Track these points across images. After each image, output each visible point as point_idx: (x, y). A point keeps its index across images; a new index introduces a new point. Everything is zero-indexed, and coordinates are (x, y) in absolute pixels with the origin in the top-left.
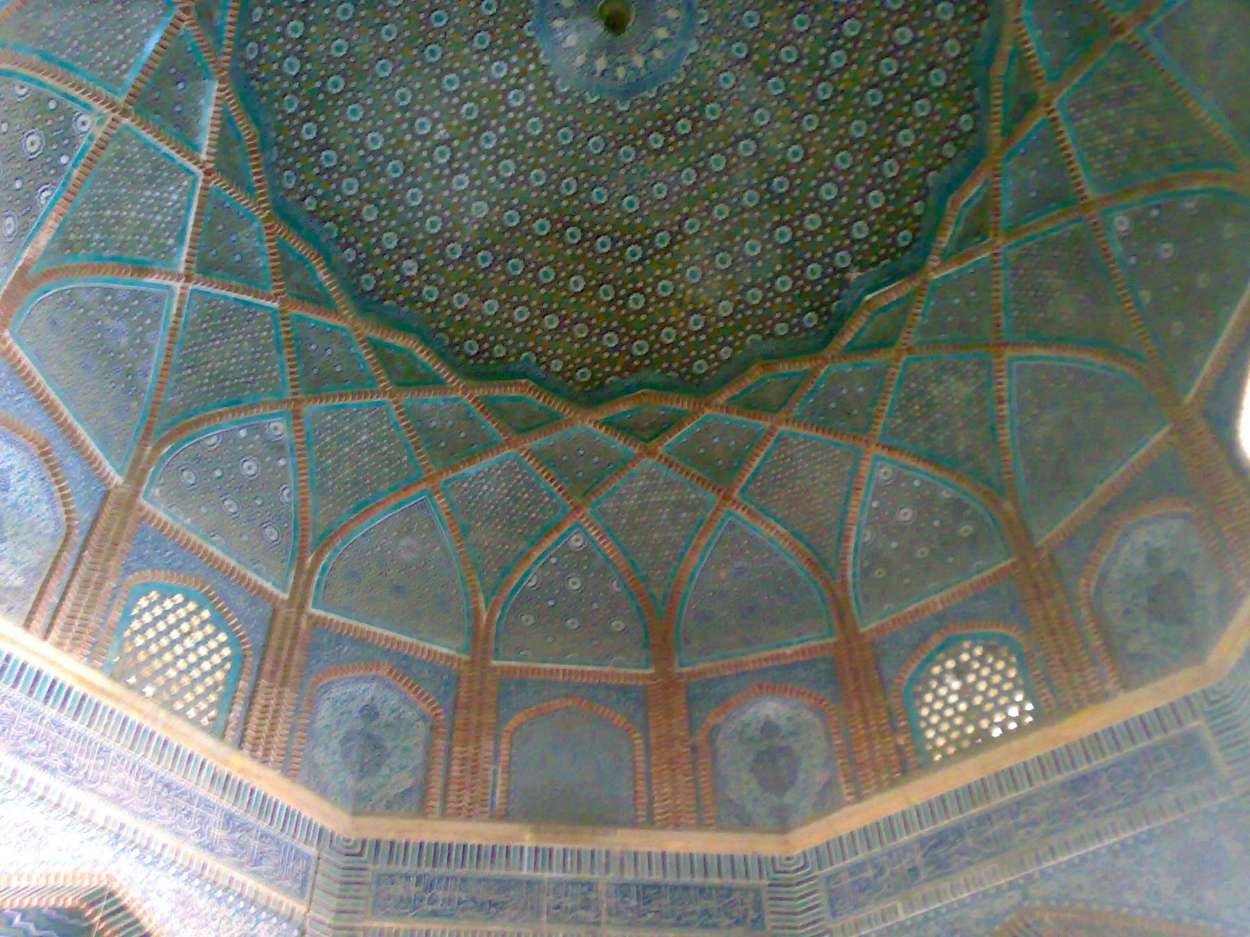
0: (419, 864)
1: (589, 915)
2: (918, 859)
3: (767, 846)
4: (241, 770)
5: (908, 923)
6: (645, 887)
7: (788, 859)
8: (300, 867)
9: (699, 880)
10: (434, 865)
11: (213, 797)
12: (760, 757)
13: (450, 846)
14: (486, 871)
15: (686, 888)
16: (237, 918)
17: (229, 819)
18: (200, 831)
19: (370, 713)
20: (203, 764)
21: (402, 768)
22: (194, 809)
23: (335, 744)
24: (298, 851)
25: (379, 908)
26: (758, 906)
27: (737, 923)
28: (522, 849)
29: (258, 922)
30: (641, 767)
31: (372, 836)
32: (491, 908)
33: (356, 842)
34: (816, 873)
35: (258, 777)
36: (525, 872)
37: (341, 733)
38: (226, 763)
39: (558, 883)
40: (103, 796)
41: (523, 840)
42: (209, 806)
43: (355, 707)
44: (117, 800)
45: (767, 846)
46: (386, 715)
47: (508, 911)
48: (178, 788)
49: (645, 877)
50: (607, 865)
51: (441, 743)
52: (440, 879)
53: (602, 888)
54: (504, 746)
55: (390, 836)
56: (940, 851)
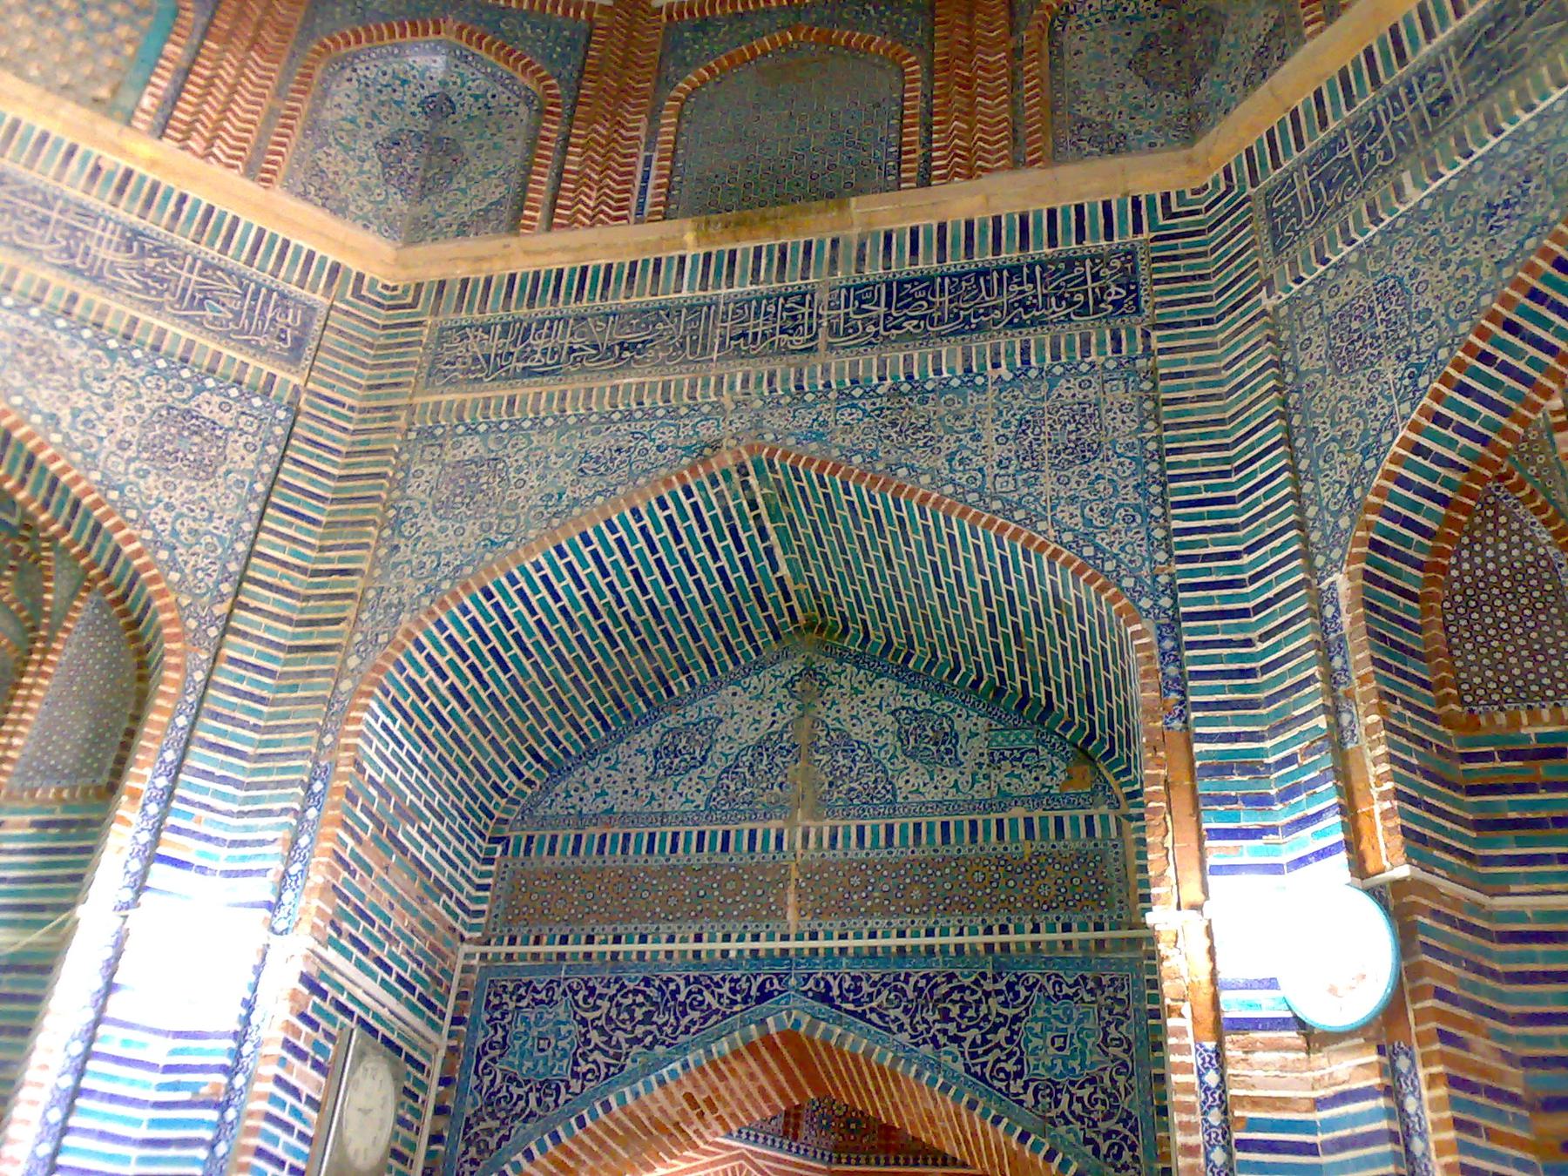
0: (506, 307)
1: (798, 341)
2: (1453, 76)
3: (1150, 174)
4: (153, 164)
5: (1426, 205)
6: (900, 283)
7: (1195, 192)
8: (293, 318)
9: (1010, 255)
10: (531, 305)
11: (98, 201)
12: (1149, 44)
13: (560, 273)
14: (619, 300)
15: (985, 272)
16: (151, 382)
17: (132, 239)
18: (68, 248)
19: (439, 106)
20: (71, 152)
21: (486, 175)
22: (55, 215)
23: (365, 147)
24: (283, 296)
25: (437, 373)
26: (1130, 284)
27: (1083, 310)
28: (682, 259)
29: (198, 392)
30: (915, 106)
31: (434, 274)
32: (626, 352)
33: (406, 291)
34: (1250, 191)
35: (194, 178)
36: (685, 293)
37: (382, 130)
38: (122, 151)
39: (742, 303)
41: (683, 246)
42: (85, 213)
43: (411, 97)
45: (1150, 174)
46: (467, 105)
47: (651, 354)
48: (17, 182)
49: (903, 267)
50: (833, 262)
51: (553, 130)
52: (542, 323)
53: (823, 296)
54: (668, 121)
55: (461, 271)
56: (1500, 43)
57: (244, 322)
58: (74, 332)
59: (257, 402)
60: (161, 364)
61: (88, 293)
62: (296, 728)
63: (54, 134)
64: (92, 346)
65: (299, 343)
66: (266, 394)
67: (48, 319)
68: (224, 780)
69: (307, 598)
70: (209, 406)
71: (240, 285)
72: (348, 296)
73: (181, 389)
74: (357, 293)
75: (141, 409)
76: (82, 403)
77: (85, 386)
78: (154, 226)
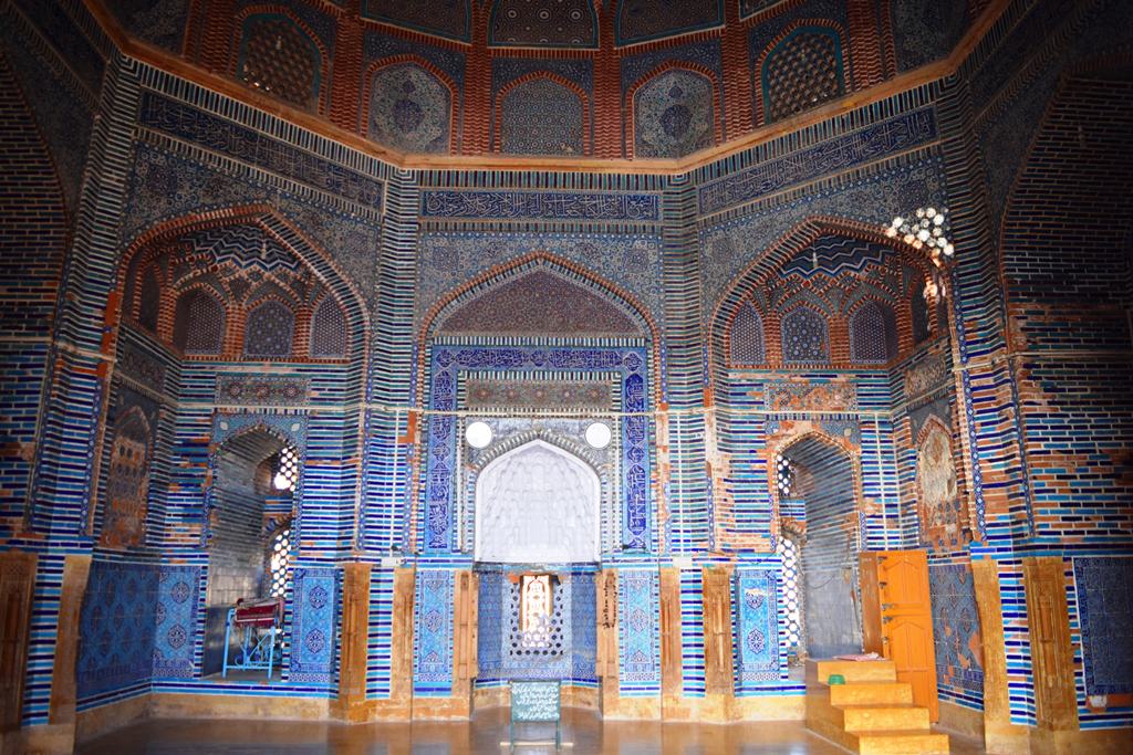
4: (856, 104)
17: (864, 135)
24: (919, 113)
29: (909, 173)
35: (869, 98)
38: (845, 109)
40: (789, 184)
42: (848, 139)
44: (797, 180)
57: (911, 135)
58: (864, 183)
59: (929, 161)
60: (894, 172)
61: (861, 167)
62: (988, 278)
63: (826, 120)
64: (871, 183)
65: (932, 127)
66: (930, 157)
67: (856, 185)
68: (977, 307)
69: (977, 224)
70: (915, 176)
71: (904, 122)
72: (941, 93)
73: (903, 177)
74: (943, 89)
75: (895, 194)
76: (878, 205)
77: (876, 199)
78: (868, 126)
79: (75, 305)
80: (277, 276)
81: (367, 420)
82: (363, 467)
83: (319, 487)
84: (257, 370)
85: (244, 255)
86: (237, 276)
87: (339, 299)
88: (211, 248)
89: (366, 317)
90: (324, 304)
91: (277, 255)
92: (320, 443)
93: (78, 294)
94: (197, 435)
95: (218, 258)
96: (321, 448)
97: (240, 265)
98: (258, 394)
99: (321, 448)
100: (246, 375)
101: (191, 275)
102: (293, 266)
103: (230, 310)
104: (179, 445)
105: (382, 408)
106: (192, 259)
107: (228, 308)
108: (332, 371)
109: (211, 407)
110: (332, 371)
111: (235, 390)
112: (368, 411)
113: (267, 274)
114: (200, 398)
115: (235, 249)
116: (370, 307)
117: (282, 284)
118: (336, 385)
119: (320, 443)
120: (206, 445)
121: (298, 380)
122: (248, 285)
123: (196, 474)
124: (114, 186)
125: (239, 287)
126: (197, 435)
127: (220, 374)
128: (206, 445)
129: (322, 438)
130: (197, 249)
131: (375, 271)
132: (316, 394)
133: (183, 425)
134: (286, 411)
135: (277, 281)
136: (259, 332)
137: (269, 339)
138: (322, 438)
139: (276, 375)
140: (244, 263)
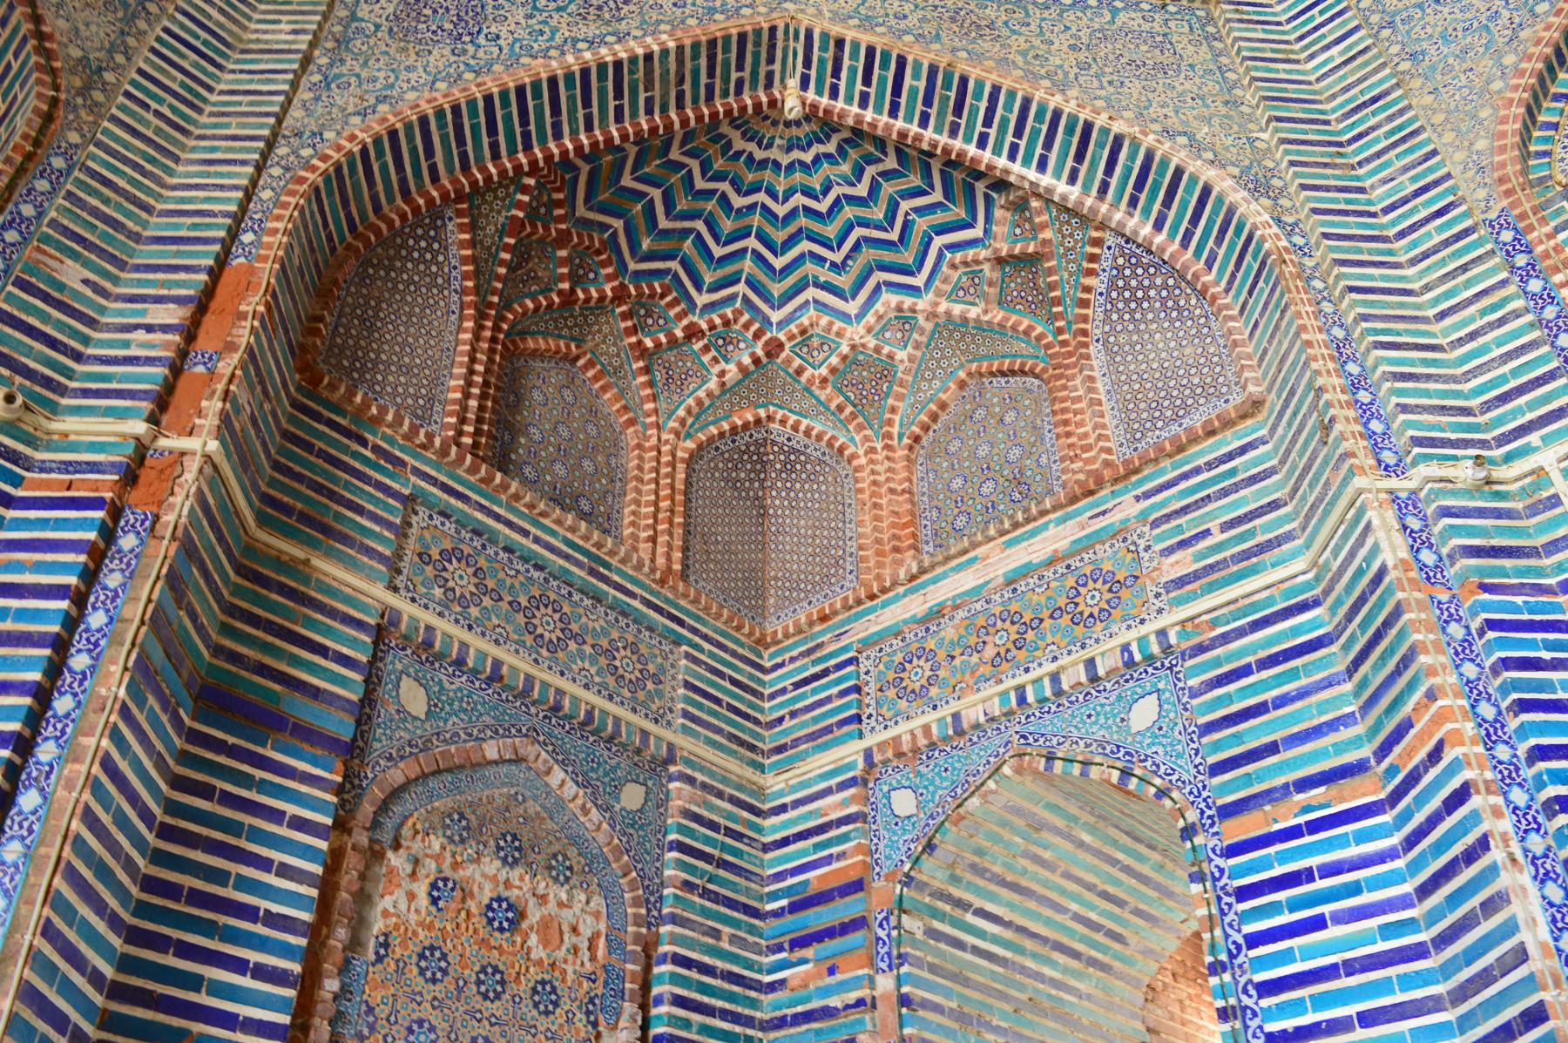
79: (61, 287)
80: (952, 297)
81: (1418, 541)
82: (1490, 741)
83: (1318, 923)
84: (967, 581)
85: (843, 281)
86: (845, 349)
87: (1147, 230)
88: (741, 288)
89: (1255, 212)
90: (1112, 285)
91: (922, 224)
92: (1254, 733)
93: (86, 264)
94: (828, 860)
95: (775, 317)
96: (1272, 749)
97: (845, 317)
98: (989, 652)
99: (1272, 749)
100: (937, 613)
101: (713, 384)
102: (977, 232)
103: (863, 461)
104: (777, 914)
105: (1465, 472)
106: (693, 333)
107: (853, 456)
108: (1210, 466)
109: (850, 752)
110: (1210, 466)
111: (917, 675)
112: (1404, 505)
113: (922, 304)
114: (821, 737)
115: (810, 267)
116: (1259, 188)
117: (973, 312)
118: (1250, 499)
119: (1254, 733)
120: (857, 886)
121: (1104, 551)
122: (886, 371)
123: (835, 1002)
124: (286, 42)
125: (865, 380)
126: (828, 860)
127: (867, 643)
128: (857, 886)
129: (1261, 709)
130: (701, 299)
131: (1235, 103)
132: (1184, 563)
133: (785, 842)
134: (1090, 664)
135: (957, 309)
136: (957, 483)
137: (988, 488)
138: (1261, 709)
139: (1026, 571)
140: (852, 307)
